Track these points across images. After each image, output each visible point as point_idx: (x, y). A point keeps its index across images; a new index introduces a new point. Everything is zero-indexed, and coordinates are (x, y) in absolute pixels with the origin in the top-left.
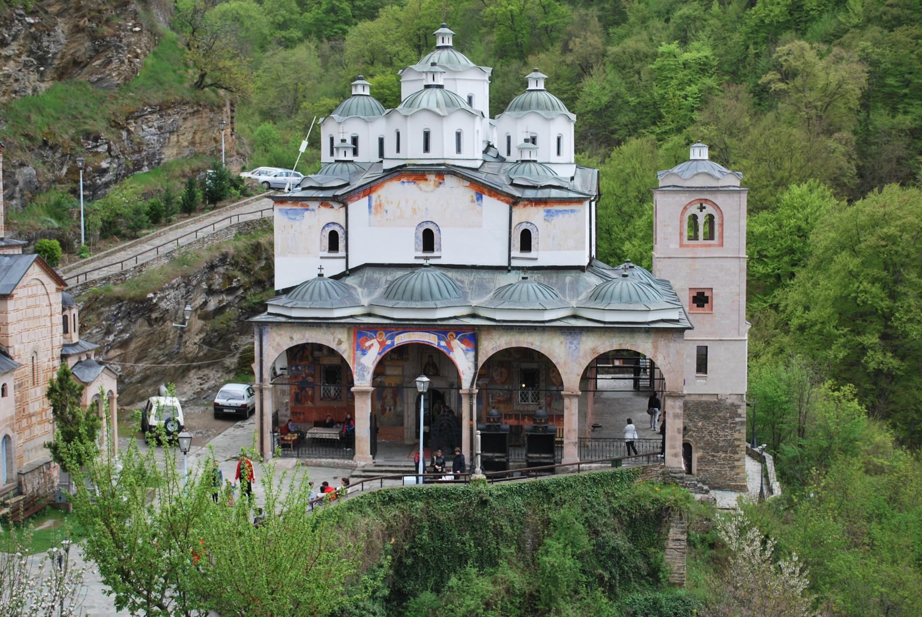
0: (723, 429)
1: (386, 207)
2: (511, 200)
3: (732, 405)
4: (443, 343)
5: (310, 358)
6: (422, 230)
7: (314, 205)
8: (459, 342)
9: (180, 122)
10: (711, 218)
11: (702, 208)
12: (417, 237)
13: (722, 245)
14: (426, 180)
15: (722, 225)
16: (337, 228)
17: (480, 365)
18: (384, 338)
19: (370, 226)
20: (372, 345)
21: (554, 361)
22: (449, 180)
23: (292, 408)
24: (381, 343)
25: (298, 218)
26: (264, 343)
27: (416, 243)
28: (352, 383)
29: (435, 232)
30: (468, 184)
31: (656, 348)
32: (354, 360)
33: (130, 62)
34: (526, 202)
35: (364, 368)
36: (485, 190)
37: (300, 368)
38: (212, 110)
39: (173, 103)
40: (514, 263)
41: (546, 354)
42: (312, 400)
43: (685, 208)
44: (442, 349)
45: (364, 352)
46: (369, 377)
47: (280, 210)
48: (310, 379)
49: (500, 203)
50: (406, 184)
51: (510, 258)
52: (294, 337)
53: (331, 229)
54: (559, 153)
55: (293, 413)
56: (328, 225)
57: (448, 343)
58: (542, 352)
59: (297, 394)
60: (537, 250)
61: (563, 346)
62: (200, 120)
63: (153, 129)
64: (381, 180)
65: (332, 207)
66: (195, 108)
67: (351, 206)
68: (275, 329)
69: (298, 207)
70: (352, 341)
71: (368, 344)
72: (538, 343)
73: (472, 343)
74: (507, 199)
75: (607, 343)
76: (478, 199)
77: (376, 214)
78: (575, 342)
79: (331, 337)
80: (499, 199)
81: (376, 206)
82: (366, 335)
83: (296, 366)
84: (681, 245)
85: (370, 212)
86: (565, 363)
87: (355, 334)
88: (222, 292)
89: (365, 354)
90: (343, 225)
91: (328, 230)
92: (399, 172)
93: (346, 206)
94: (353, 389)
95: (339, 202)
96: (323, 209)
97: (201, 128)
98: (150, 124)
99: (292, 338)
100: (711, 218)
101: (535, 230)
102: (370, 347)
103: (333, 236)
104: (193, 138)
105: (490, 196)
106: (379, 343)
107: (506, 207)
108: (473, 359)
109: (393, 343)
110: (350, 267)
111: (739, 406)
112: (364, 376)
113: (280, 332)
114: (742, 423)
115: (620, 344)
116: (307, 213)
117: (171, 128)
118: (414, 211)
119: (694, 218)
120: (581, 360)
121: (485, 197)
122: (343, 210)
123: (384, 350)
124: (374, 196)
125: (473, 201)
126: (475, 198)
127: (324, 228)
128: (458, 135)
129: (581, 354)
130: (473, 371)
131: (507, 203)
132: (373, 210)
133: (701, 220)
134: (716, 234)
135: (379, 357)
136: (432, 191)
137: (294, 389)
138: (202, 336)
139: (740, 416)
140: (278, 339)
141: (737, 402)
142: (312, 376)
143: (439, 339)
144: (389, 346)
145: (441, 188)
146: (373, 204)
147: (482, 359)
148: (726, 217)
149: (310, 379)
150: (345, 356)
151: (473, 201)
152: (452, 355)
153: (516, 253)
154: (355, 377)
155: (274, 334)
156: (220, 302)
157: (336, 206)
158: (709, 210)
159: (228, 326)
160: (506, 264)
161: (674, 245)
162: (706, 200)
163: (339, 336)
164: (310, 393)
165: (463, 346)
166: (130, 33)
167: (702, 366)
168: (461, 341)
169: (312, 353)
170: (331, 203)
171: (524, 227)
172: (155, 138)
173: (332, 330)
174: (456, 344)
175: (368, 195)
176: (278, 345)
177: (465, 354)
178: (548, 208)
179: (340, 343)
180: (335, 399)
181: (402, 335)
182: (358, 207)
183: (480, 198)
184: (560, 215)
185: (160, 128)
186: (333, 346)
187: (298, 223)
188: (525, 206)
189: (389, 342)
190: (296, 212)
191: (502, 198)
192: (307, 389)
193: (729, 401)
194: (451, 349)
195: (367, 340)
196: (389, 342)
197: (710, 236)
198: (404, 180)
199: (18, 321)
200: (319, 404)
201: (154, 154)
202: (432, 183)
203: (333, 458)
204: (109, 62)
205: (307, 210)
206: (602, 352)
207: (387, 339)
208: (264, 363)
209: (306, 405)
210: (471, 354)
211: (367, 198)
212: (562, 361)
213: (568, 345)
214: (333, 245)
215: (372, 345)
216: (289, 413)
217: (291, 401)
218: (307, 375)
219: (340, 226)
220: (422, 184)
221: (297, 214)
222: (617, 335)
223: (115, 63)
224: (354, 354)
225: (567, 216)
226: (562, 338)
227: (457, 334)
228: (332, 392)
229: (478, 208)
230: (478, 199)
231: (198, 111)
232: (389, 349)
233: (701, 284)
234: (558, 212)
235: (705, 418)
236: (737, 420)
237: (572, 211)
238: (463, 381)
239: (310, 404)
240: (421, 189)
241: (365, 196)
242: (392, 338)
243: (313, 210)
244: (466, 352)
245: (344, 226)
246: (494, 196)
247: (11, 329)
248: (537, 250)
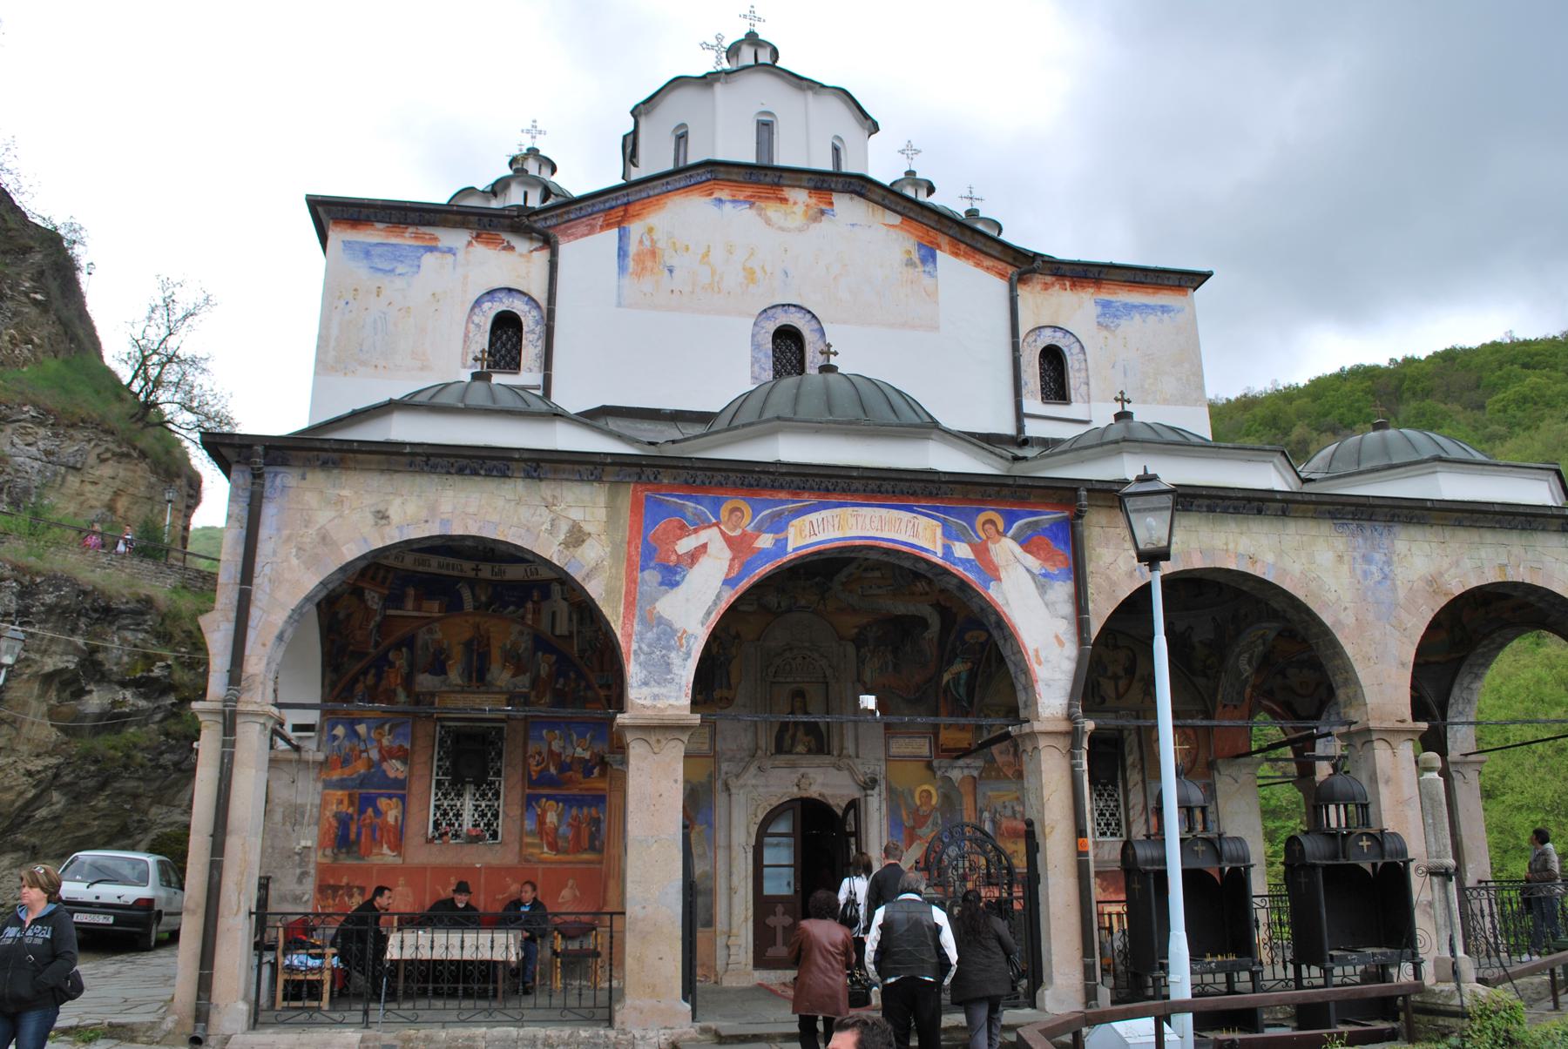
2: (1010, 270)
4: (962, 550)
5: (402, 696)
6: (771, 327)
7: (455, 238)
8: (1018, 550)
9: (92, 459)
12: (756, 346)
14: (784, 200)
16: (518, 306)
17: (1095, 629)
18: (747, 523)
19: (619, 305)
20: (705, 546)
21: (1327, 618)
22: (847, 208)
23: (323, 870)
25: (401, 269)
26: (264, 533)
27: (755, 361)
28: (617, 699)
30: (896, 220)
32: (630, 604)
34: (1049, 279)
35: (668, 634)
36: (943, 240)
37: (361, 729)
38: (154, 472)
39: (83, 421)
40: (1033, 429)
41: (1300, 594)
42: (398, 845)
44: (959, 570)
45: (671, 576)
46: (686, 672)
47: (347, 245)
48: (395, 769)
49: (979, 272)
50: (728, 207)
51: (1020, 415)
52: (395, 512)
53: (499, 307)
56: (491, 293)
57: (981, 550)
58: (1287, 586)
59: (343, 822)
60: (1088, 399)
61: (1345, 568)
62: (129, 474)
63: (33, 450)
64: (658, 187)
65: (510, 248)
66: (124, 449)
67: (569, 250)
68: (317, 478)
69: (405, 239)
70: (624, 533)
71: (685, 545)
72: (1270, 558)
73: (1063, 553)
74: (1001, 265)
75: (1467, 564)
76: (924, 261)
77: (638, 275)
78: (1379, 557)
79: (545, 517)
80: (978, 265)
81: (640, 258)
82: (680, 511)
83: (351, 724)
85: (622, 268)
87: (636, 506)
88: (124, 685)
89: (677, 584)
90: (539, 292)
91: (492, 309)
92: (716, 173)
93: (549, 243)
94: (621, 719)
96: (480, 250)
97: (131, 490)
98: (30, 439)
99: (382, 516)
101: (1076, 348)
102: (695, 556)
103: (507, 325)
104: (113, 500)
105: (956, 255)
106: (729, 541)
107: (999, 287)
108: (1068, 609)
109: (781, 545)
112: (668, 666)
113: (332, 492)
115: (1502, 567)
116: (429, 260)
117: (72, 460)
118: (750, 275)
120: (1404, 615)
121: (943, 257)
122: (542, 257)
123: (746, 568)
124: (636, 228)
125: (910, 263)
126: (915, 256)
127: (478, 303)
129: (1401, 593)
130: (1071, 650)
131: (1002, 276)
132: (631, 264)
135: (729, 597)
136: (800, 230)
137: (338, 802)
138: (53, 761)
140: (324, 517)
142: (404, 756)
144: (765, 555)
145: (825, 225)
146: (633, 248)
147: (1101, 610)
149: (395, 769)
150: (595, 589)
151: (910, 263)
152: (994, 593)
153: (1033, 404)
154: (634, 671)
155: (311, 499)
156: (114, 703)
157: (522, 245)
159: (128, 757)
160: (1008, 428)
163: (576, 514)
164: (392, 816)
165: (1032, 561)
166: (24, 299)
168: (1026, 543)
169: (408, 682)
170: (506, 237)
171: (1047, 338)
172: (37, 465)
173: (547, 489)
174: (1006, 550)
175: (619, 224)
176: (324, 539)
177: (1042, 589)
178: (1104, 296)
179: (577, 537)
180: (474, 839)
181: (814, 517)
183: (928, 256)
184: (1137, 317)
185: (48, 453)
186: (551, 549)
187: (399, 283)
188: (1046, 287)
189: (765, 541)
190: (397, 255)
191: (988, 262)
192: (383, 803)
194: (991, 572)
195: (683, 531)
196: (765, 541)
198: (724, 194)
200: (420, 854)
201: (26, 491)
202: (800, 209)
203: (519, 1022)
205: (432, 249)
206: (1457, 591)
207: (760, 530)
208: (255, 613)
209: (375, 860)
210: (1063, 590)
211: (613, 233)
212: (1348, 619)
213: (1360, 567)
215: (705, 546)
216: (309, 887)
217: (322, 846)
218: (387, 755)
219: (531, 299)
220: (773, 211)
221: (399, 259)
222: (1489, 536)
224: (632, 581)
225: (1152, 319)
227: (1010, 519)
229: (927, 280)
230: (924, 261)
231: (128, 455)
232: (767, 568)
234: (1130, 308)
237: (1164, 309)
238: (1040, 688)
239: (387, 856)
240: (768, 222)
241: (607, 225)
242: (778, 524)
243: (451, 251)
244: (1042, 582)
245: (543, 304)
246: (966, 256)
248: (1088, 399)
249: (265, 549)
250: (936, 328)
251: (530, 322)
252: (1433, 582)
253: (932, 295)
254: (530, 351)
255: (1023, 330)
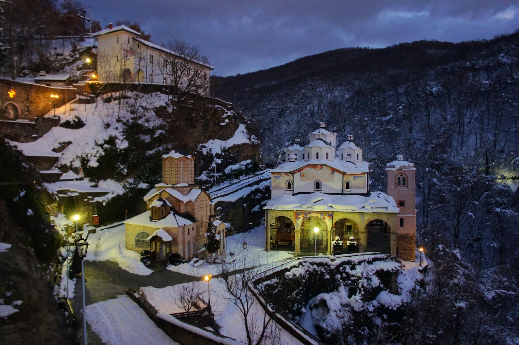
0: (408, 244)
1: (305, 175)
3: (411, 236)
10: (404, 179)
11: (401, 175)
12: (314, 184)
13: (408, 187)
15: (407, 181)
16: (290, 182)
23: (276, 236)
24: (303, 217)
29: (320, 183)
31: (388, 219)
33: (230, 132)
35: (298, 224)
40: (344, 192)
43: (396, 176)
45: (298, 219)
46: (300, 227)
51: (343, 191)
54: (357, 159)
55: (276, 237)
56: (287, 181)
57: (324, 217)
59: (278, 231)
71: (299, 217)
77: (302, 177)
84: (395, 187)
86: (360, 223)
90: (292, 180)
95: (291, 173)
100: (404, 179)
103: (289, 184)
107: (342, 175)
108: (331, 222)
110: (294, 193)
111: (413, 237)
114: (414, 242)
116: (281, 177)
118: (314, 176)
119: (399, 178)
124: (301, 172)
128: (327, 154)
130: (331, 225)
133: (401, 179)
134: (406, 183)
139: (413, 240)
141: (413, 236)
143: (321, 215)
147: (334, 222)
148: (409, 178)
150: (292, 220)
157: (290, 175)
158: (404, 176)
160: (341, 192)
161: (393, 187)
162: (403, 173)
167: (402, 224)
169: (282, 219)
171: (347, 182)
179: (291, 216)
182: (297, 176)
183: (333, 172)
186: (289, 217)
193: (410, 235)
196: (306, 216)
197: (404, 184)
199: (197, 208)
204: (224, 132)
210: (332, 220)
212: (359, 223)
214: (289, 187)
220: (316, 169)
223: (226, 133)
225: (360, 178)
226: (359, 216)
228: (288, 231)
233: (401, 199)
235: (403, 240)
236: (413, 241)
237: (362, 177)
244: (329, 220)
247: (195, 211)
249: (268, 217)
250: (334, 181)
251: (291, 183)
252: (369, 220)
253: (334, 177)
254: (291, 187)
255: (344, 181)
